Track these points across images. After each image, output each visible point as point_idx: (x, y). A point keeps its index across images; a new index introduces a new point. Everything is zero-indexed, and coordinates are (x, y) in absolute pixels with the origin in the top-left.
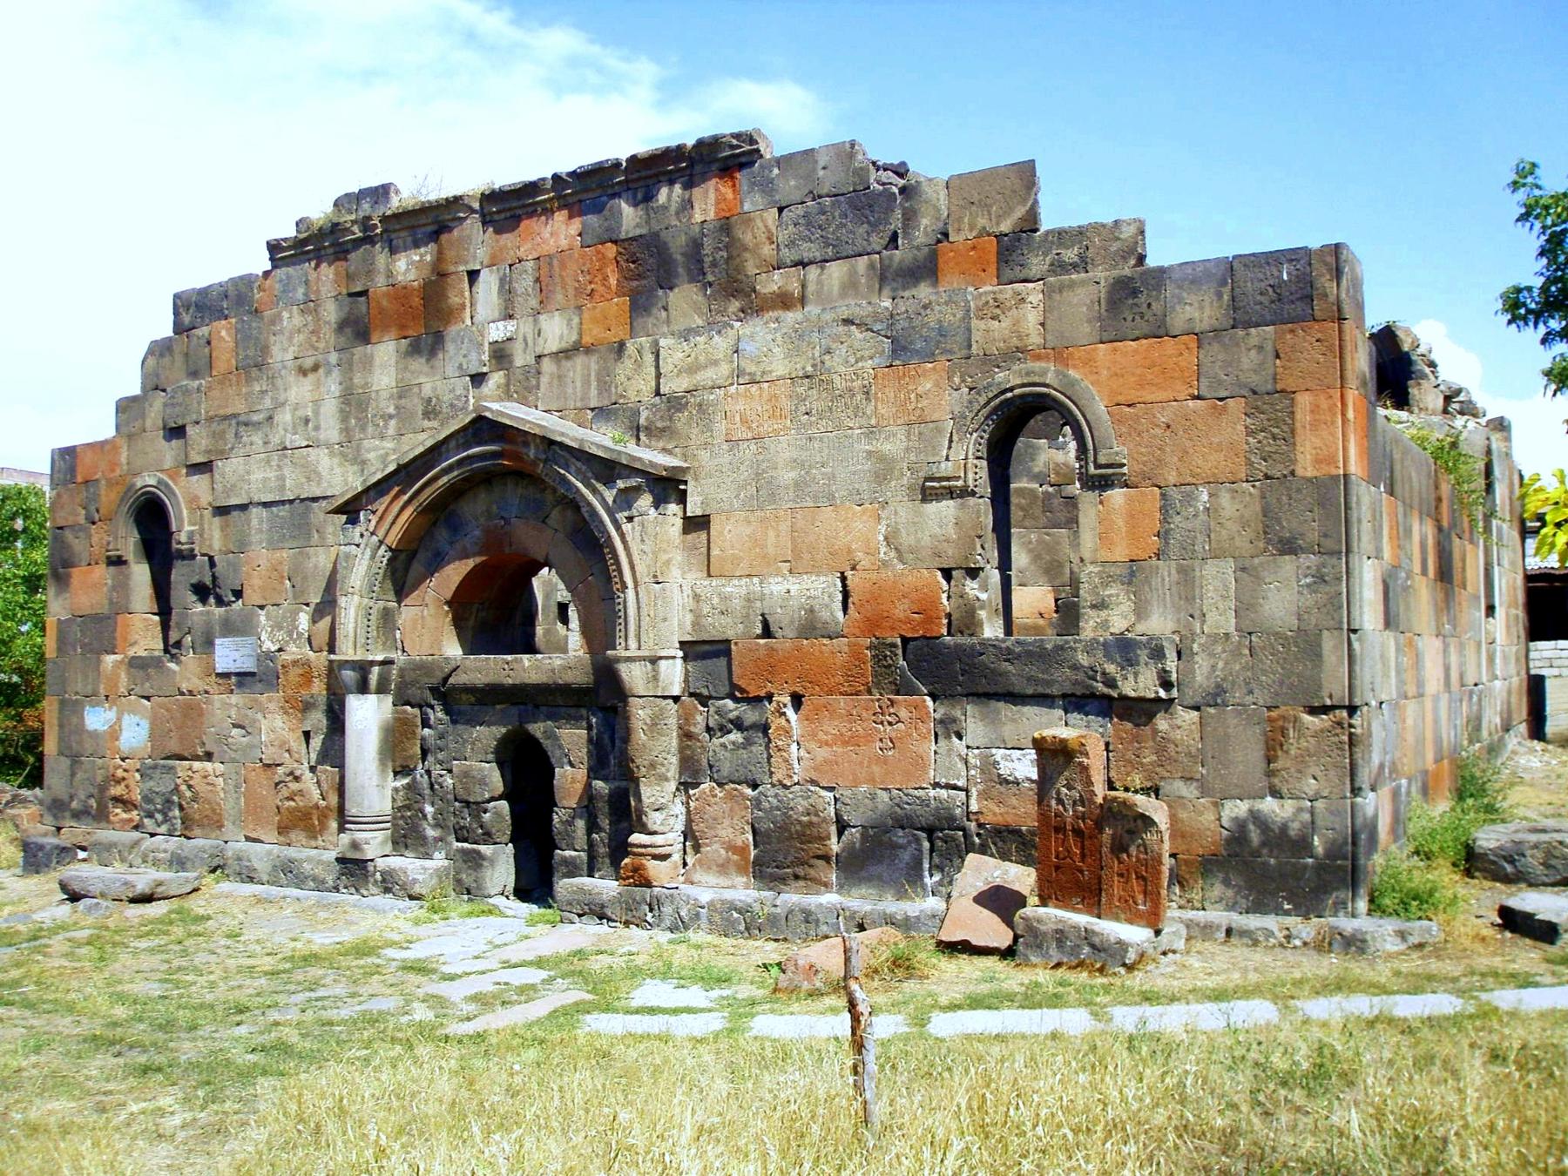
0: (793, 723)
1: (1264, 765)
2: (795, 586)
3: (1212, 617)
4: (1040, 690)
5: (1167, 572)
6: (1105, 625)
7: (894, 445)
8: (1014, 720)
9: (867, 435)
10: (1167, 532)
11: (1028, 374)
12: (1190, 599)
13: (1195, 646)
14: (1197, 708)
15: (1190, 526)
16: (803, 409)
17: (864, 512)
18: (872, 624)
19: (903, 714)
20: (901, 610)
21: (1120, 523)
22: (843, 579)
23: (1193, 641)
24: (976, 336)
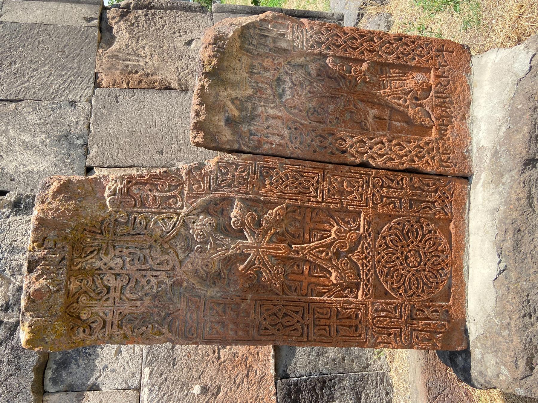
1: (173, 93)
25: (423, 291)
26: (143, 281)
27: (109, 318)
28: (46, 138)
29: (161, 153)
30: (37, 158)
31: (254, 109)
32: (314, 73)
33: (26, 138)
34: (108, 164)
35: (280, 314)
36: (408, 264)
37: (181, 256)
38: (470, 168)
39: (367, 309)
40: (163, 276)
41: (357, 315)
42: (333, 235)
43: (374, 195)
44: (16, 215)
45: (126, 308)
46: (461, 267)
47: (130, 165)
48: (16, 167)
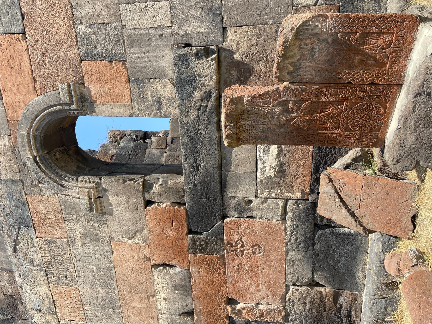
0: (245, 306)
2: (161, 295)
3: (161, 20)
4: (215, 146)
5: (133, 54)
6: (171, 100)
7: (77, 230)
8: (237, 166)
9: (73, 244)
10: (108, 55)
11: (24, 146)
12: (150, 37)
13: (181, 33)
14: (224, 29)
15: (101, 38)
16: (64, 279)
17: (117, 250)
18: (180, 252)
19: (236, 237)
20: (171, 233)
21: (106, 88)
22: (155, 266)
23: (177, 34)
24: (10, 176)
25: (367, 129)
26: (258, 128)
27: (248, 138)
28: (202, 11)
29: (260, 15)
30: (200, 24)
31: (300, 64)
32: (330, 42)
33: (193, 12)
34: (233, 25)
35: (306, 137)
36: (363, 120)
37: (270, 120)
38: (403, 81)
39: (341, 135)
40: (264, 126)
41: (337, 137)
42: (331, 111)
43: (351, 95)
44: (198, 60)
45: (253, 135)
46: (388, 120)
47: (244, 25)
48: (192, 30)
